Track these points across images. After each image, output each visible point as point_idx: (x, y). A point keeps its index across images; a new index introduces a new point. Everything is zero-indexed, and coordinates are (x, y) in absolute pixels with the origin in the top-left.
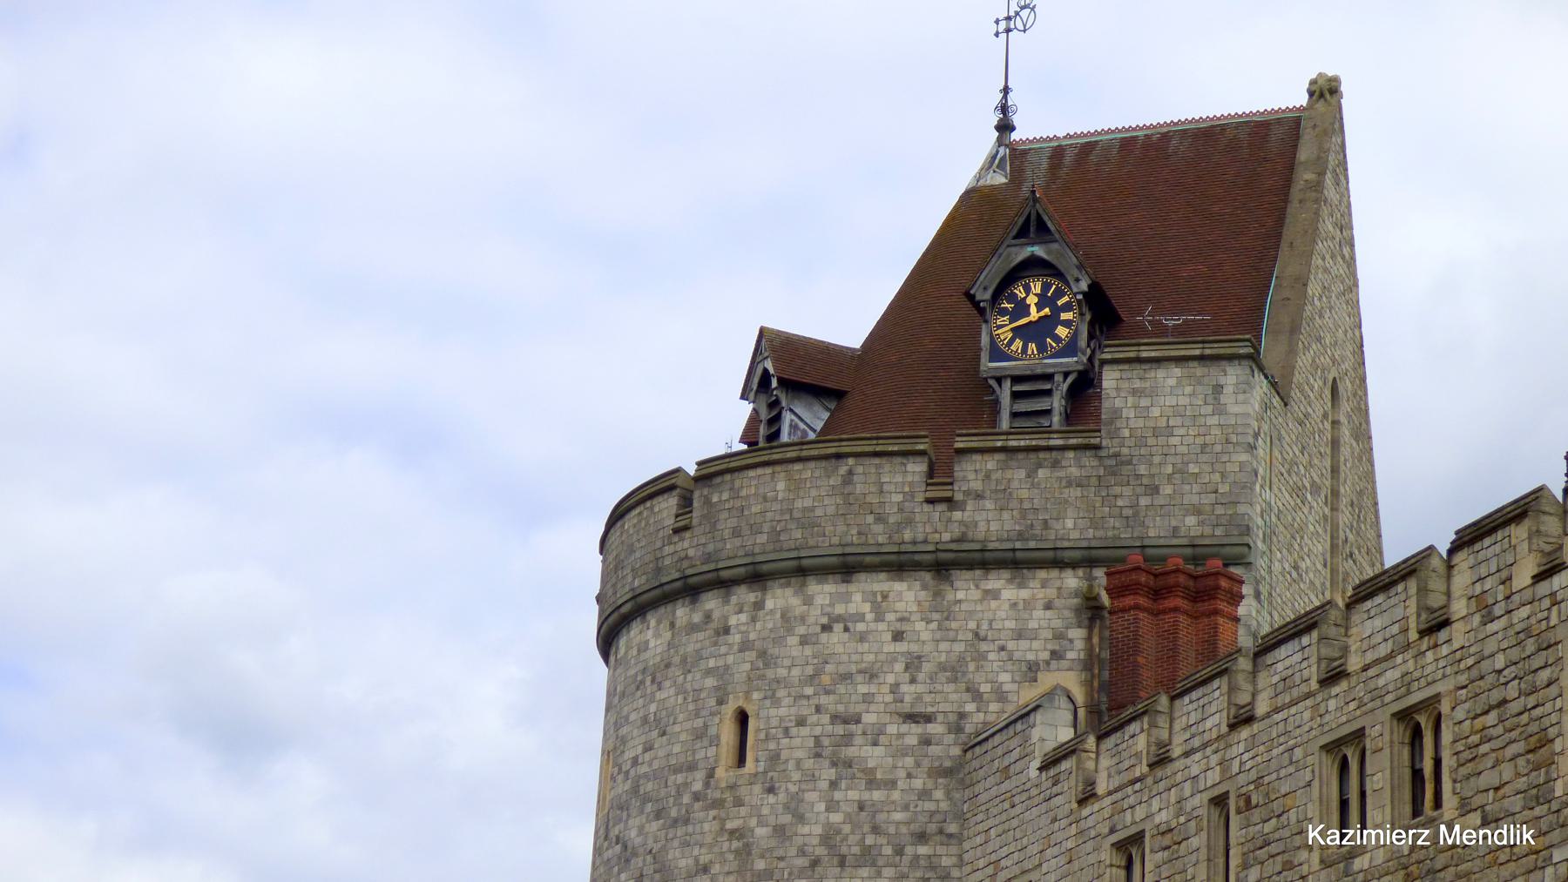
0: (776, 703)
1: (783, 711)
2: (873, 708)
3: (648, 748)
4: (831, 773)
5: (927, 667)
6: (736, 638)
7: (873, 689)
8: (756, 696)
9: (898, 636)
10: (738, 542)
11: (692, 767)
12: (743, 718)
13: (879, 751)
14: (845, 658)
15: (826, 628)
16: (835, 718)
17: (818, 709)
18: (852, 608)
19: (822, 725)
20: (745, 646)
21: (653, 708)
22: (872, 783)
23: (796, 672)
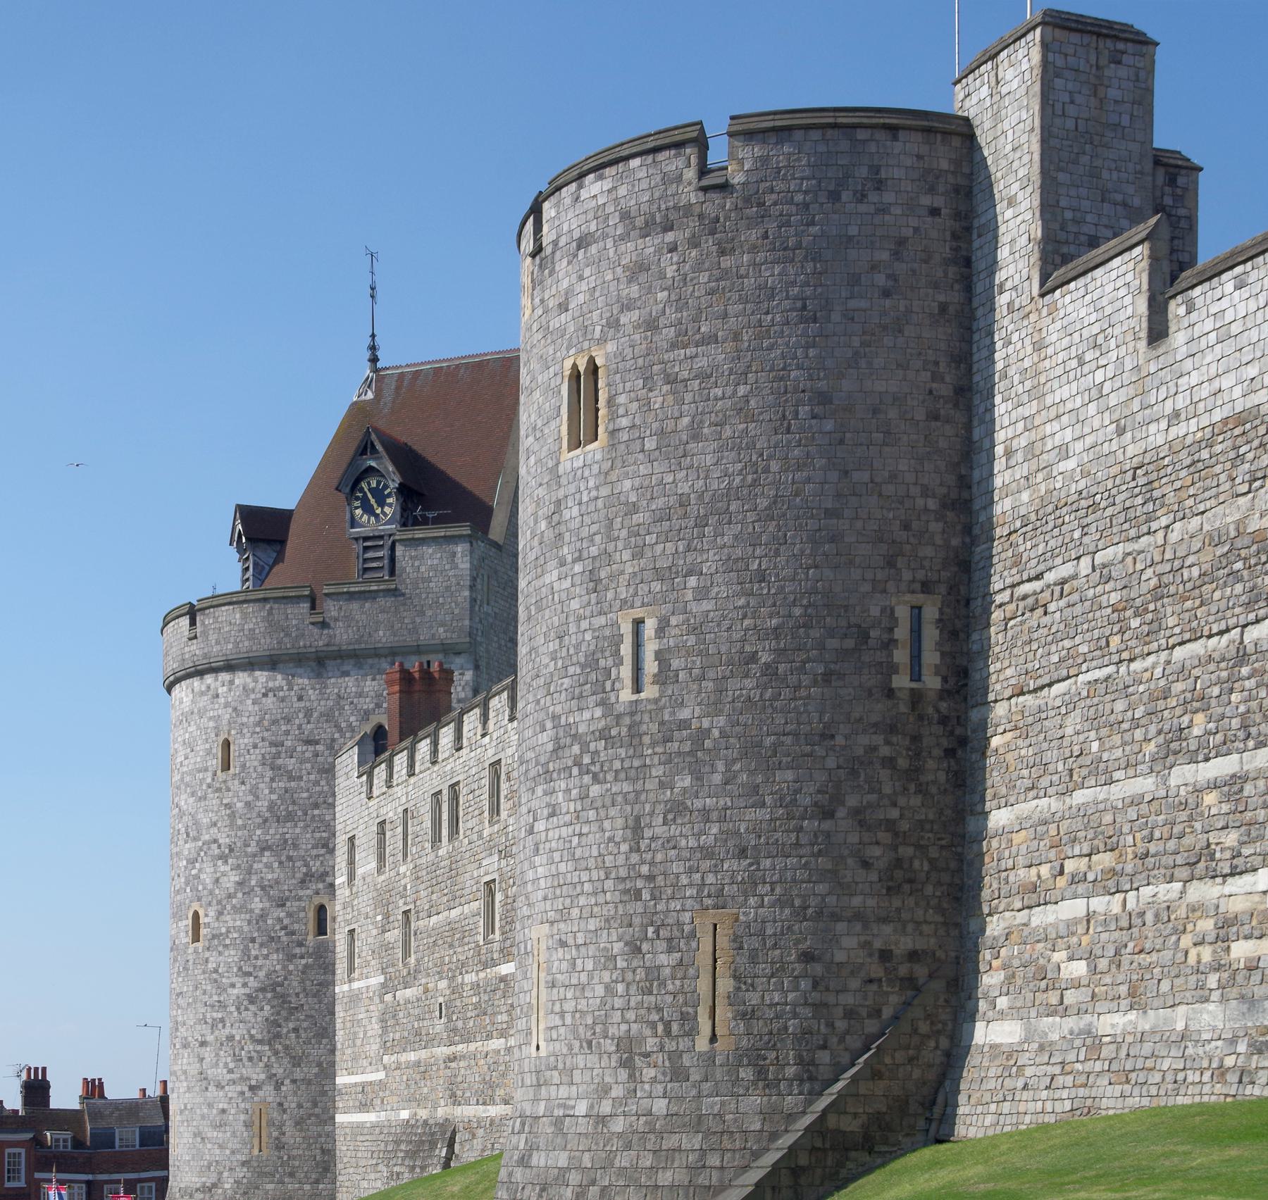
0: (243, 736)
1: (246, 741)
2: (289, 738)
3: (186, 758)
4: (269, 774)
5: (315, 715)
6: (222, 700)
7: (289, 727)
8: (233, 732)
9: (300, 699)
10: (219, 647)
11: (206, 770)
12: (227, 744)
13: (293, 760)
14: (274, 711)
15: (265, 695)
16: (272, 744)
17: (263, 739)
18: (277, 684)
19: (264, 748)
20: (227, 705)
21: (187, 736)
22: (291, 778)
23: (252, 719)
